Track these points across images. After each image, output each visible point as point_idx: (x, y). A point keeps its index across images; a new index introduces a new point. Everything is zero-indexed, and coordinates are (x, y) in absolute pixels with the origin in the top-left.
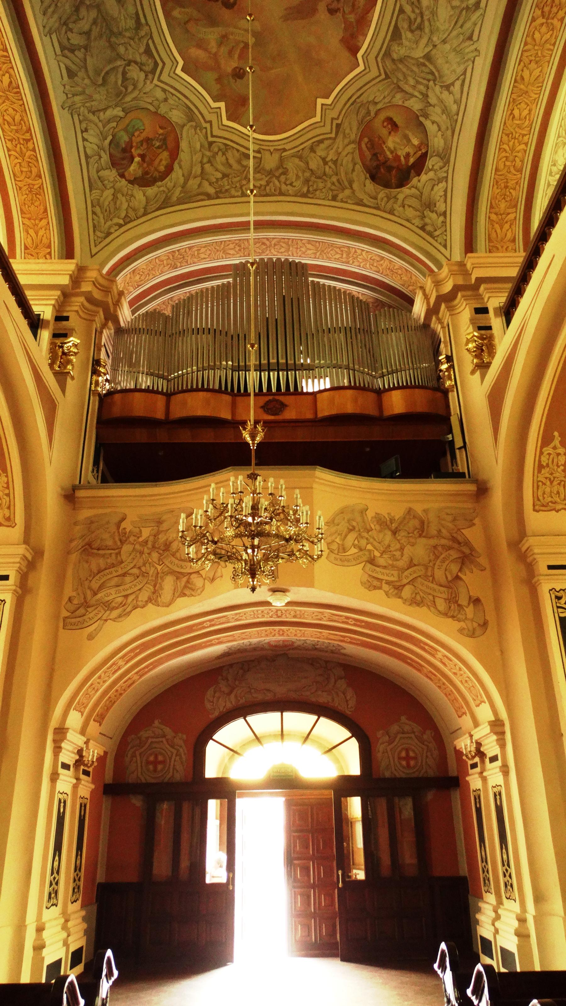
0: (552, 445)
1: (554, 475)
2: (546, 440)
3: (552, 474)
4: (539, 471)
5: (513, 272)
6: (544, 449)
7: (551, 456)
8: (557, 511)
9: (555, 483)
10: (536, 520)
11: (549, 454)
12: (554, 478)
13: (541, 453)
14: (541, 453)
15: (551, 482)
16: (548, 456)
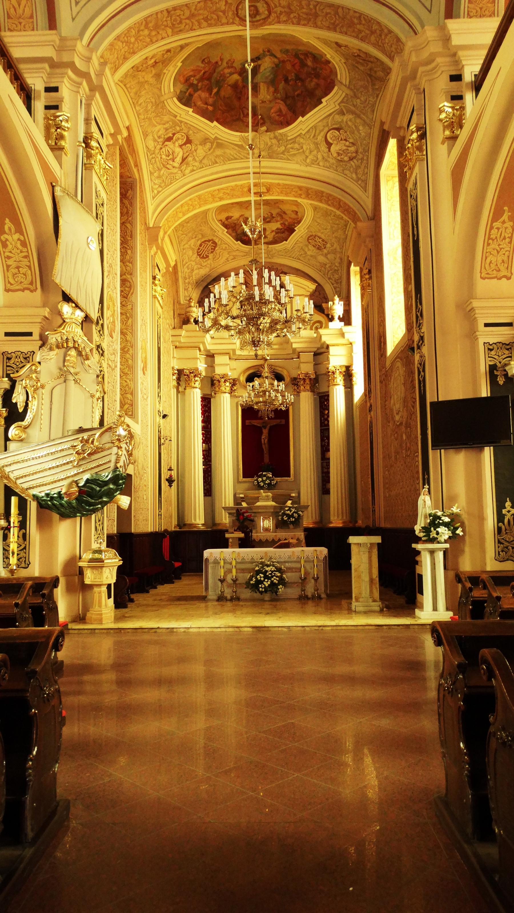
0: (502, 220)
1: (501, 247)
2: (497, 215)
3: (499, 245)
4: (489, 244)
5: (488, 39)
6: (494, 224)
7: (500, 230)
8: (500, 279)
9: (501, 253)
10: (482, 286)
11: (498, 229)
12: (501, 249)
13: (492, 228)
14: (492, 228)
15: (498, 252)
16: (496, 230)
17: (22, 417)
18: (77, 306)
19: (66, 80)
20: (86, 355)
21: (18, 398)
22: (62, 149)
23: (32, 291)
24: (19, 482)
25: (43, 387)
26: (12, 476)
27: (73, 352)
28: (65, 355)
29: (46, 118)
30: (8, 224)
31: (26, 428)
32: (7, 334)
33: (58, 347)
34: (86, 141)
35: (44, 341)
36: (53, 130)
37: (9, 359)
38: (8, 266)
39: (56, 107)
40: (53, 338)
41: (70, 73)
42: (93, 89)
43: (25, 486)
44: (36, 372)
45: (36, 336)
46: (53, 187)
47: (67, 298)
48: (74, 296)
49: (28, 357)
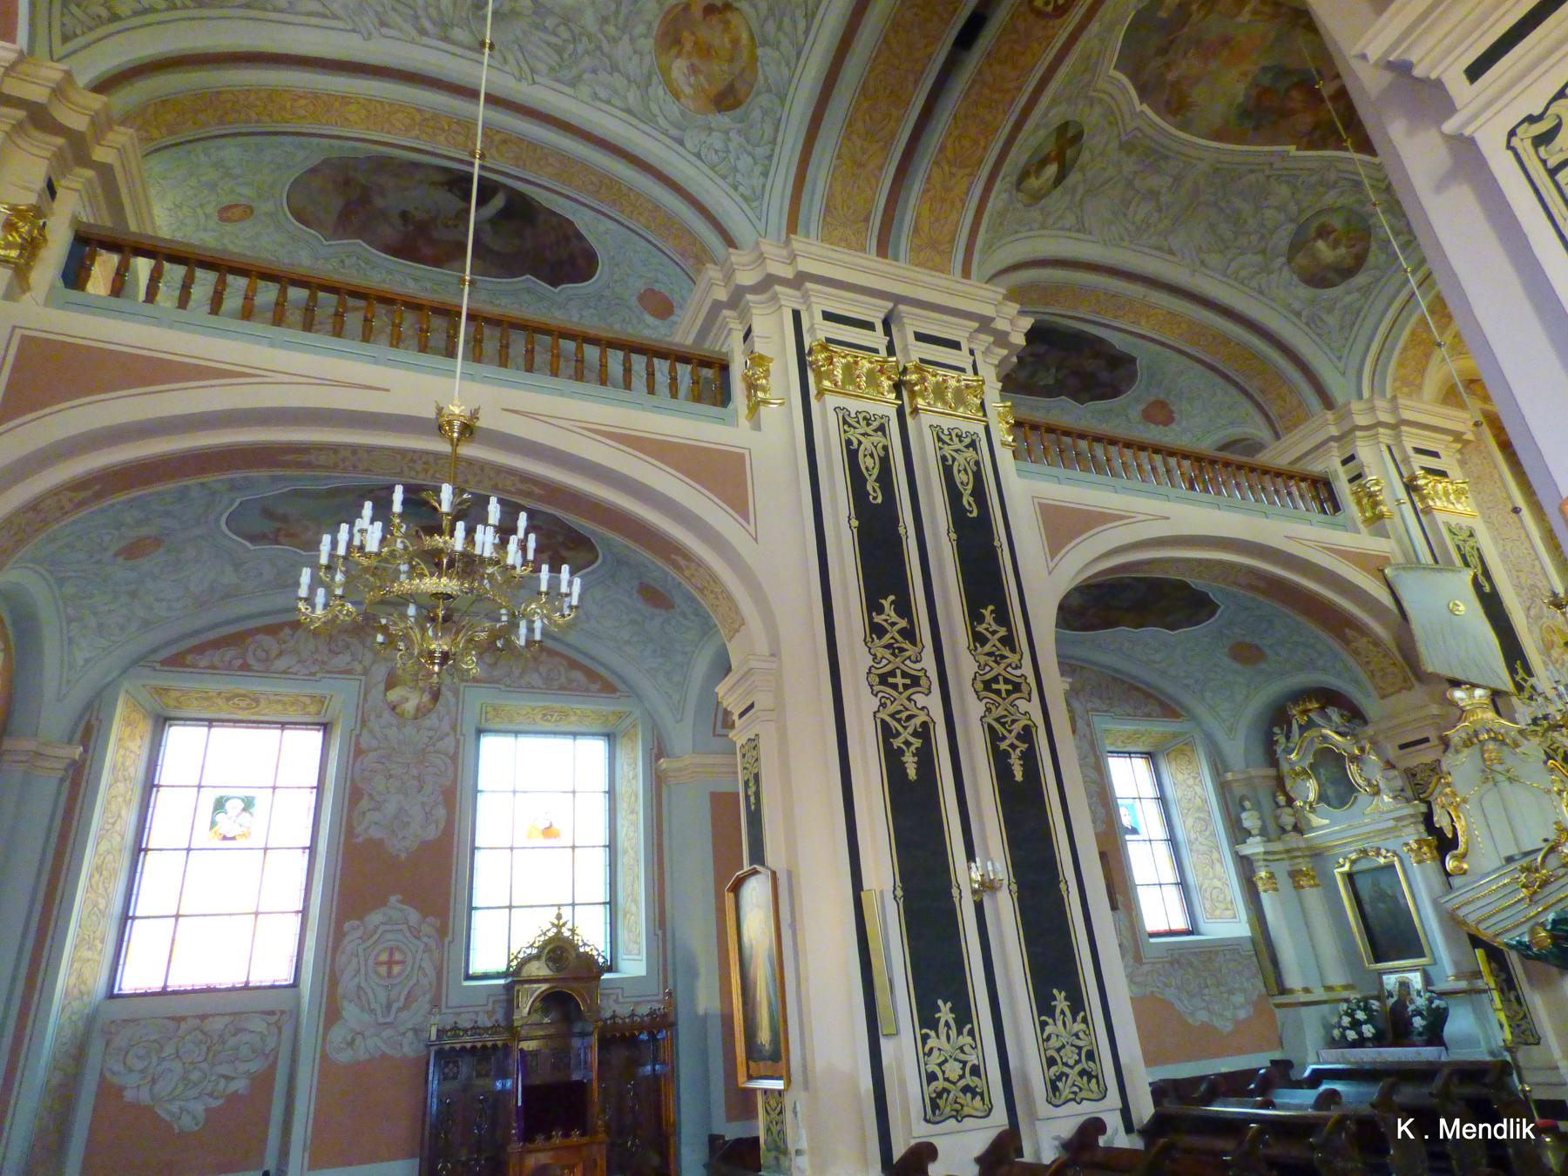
17: (1453, 843)
18: (1474, 686)
19: (1359, 443)
20: (1514, 741)
21: (1441, 820)
22: (1381, 516)
23: (1409, 689)
24: (1482, 926)
25: (1464, 801)
26: (1471, 919)
27: (1491, 746)
28: (1483, 752)
29: (1355, 493)
30: (1349, 633)
31: (1464, 856)
32: (1402, 747)
33: (1466, 746)
34: (1411, 487)
35: (1446, 743)
36: (1365, 501)
37: (1414, 775)
38: (1372, 672)
39: (1359, 476)
40: (1455, 735)
41: (1358, 433)
42: (1394, 427)
43: (1490, 932)
44: (1448, 785)
45: (1434, 741)
46: (1382, 571)
47: (1456, 684)
48: (1460, 676)
49: (1435, 769)
